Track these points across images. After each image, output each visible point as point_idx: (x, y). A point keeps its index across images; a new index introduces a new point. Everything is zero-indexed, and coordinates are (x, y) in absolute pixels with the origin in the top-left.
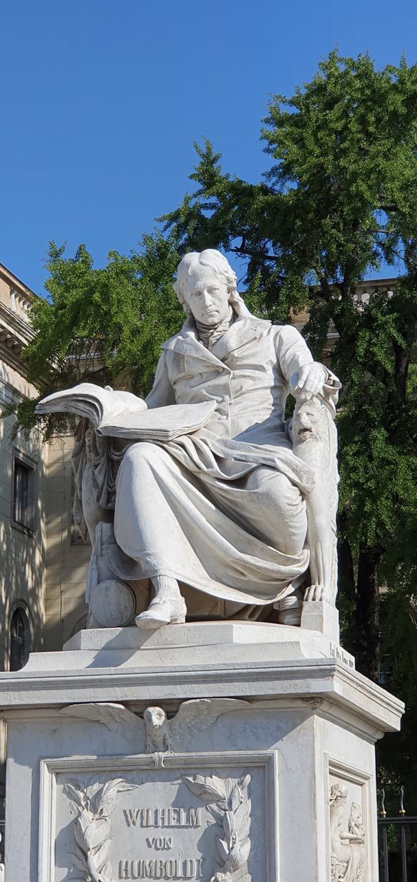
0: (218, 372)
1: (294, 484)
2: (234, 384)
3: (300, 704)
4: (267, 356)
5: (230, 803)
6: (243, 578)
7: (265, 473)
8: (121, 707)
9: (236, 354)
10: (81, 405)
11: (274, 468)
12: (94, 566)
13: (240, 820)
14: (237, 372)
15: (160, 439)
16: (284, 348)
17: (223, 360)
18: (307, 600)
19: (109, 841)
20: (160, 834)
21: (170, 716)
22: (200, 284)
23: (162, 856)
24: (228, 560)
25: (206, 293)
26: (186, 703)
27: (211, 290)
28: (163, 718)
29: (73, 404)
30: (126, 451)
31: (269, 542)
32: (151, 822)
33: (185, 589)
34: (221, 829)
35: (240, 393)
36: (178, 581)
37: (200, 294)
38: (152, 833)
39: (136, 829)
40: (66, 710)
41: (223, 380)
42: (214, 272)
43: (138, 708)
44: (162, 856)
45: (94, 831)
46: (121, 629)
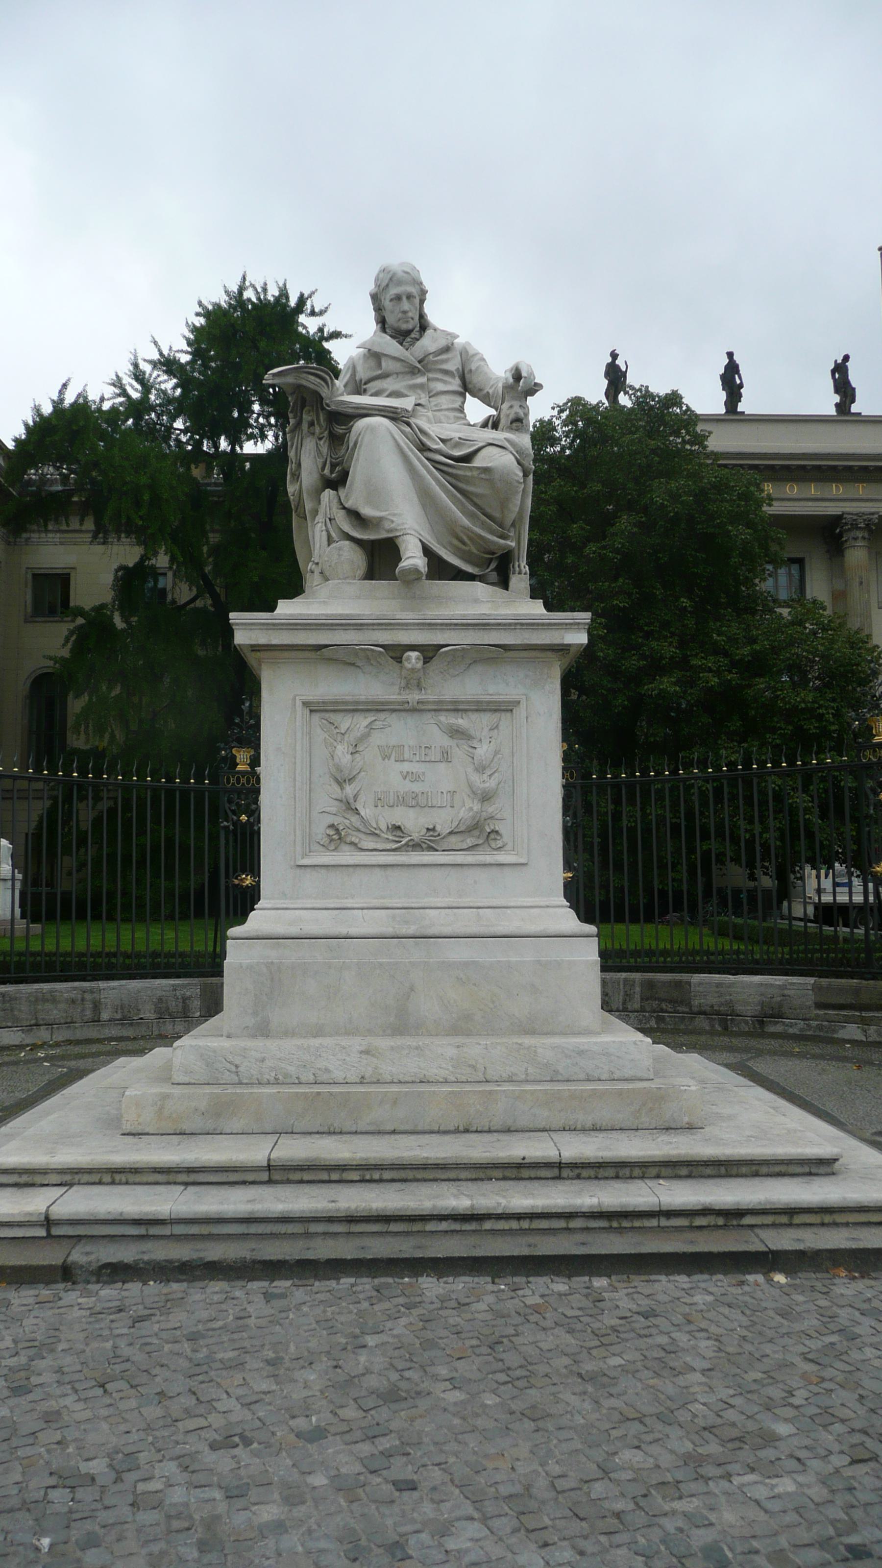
1: (519, 463)
3: (549, 654)
6: (464, 547)
8: (381, 649)
10: (312, 378)
12: (324, 528)
14: (431, 375)
17: (420, 362)
18: (514, 573)
19: (363, 773)
21: (427, 660)
25: (404, 298)
26: (444, 649)
27: (409, 297)
28: (422, 662)
29: (305, 375)
30: (352, 426)
33: (427, 551)
38: (406, 767)
43: (397, 652)
44: (416, 787)
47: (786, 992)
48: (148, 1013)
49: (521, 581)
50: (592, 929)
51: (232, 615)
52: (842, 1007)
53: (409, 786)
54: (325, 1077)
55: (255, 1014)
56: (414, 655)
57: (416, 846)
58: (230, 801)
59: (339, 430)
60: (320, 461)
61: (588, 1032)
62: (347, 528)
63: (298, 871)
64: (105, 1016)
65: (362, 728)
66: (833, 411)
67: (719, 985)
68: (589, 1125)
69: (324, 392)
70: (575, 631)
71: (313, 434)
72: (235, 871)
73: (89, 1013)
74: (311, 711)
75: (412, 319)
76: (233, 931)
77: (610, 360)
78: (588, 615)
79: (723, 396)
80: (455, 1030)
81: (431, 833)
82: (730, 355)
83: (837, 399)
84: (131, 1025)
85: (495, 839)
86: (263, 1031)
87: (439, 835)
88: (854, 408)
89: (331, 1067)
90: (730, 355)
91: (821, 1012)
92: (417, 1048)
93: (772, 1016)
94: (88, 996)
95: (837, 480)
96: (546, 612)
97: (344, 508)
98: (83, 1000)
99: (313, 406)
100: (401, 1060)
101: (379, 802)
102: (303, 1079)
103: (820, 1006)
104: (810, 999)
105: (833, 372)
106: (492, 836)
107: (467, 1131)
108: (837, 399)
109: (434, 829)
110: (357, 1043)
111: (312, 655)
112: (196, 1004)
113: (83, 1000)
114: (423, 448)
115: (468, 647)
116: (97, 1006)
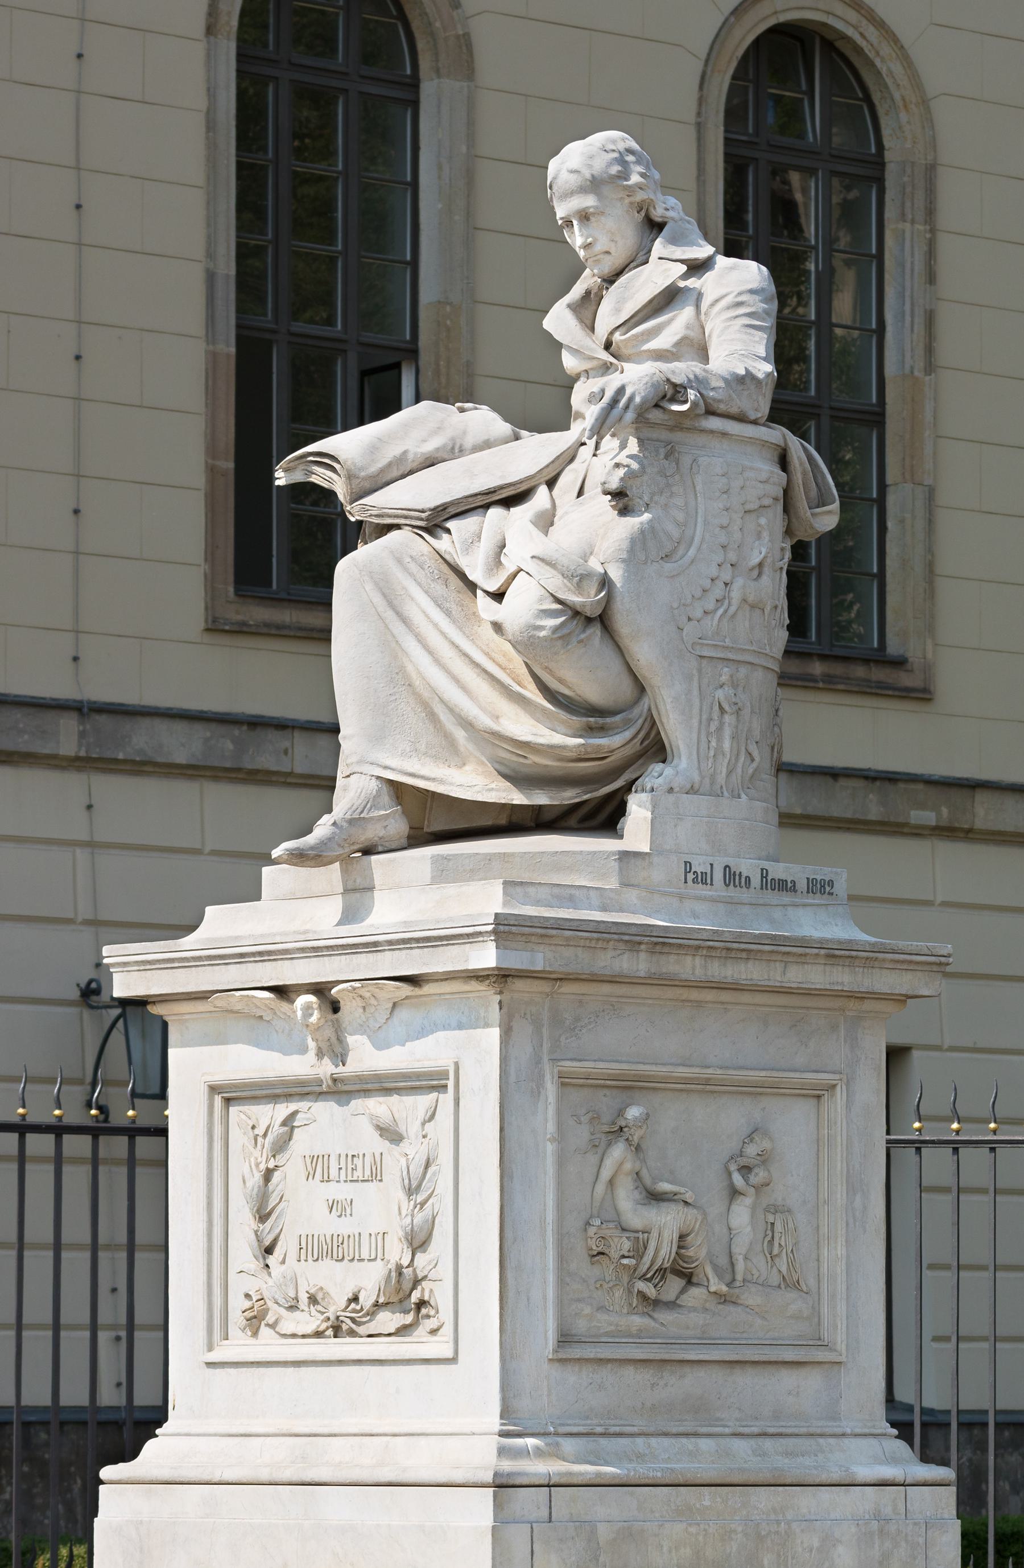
36: (391, 782)
44: (344, 1227)
51: (106, 950)
63: (211, 1371)
65: (276, 1127)
74: (228, 1101)
75: (608, 253)
81: (353, 1305)
85: (428, 1316)
87: (362, 1309)
106: (424, 1311)
109: (355, 1299)
115: (357, 984)
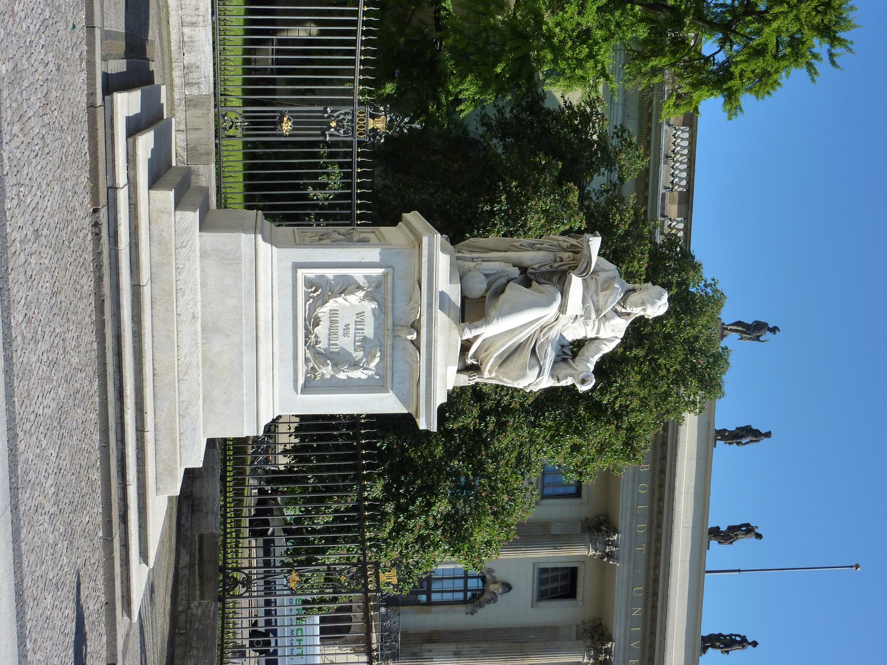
0: (598, 311)
2: (590, 322)
4: (602, 335)
5: (366, 369)
7: (536, 370)
9: (607, 323)
10: (585, 265)
11: (538, 376)
13: (358, 374)
14: (597, 322)
15: (563, 309)
16: (607, 343)
20: (352, 331)
22: (649, 306)
23: (341, 332)
24: (492, 349)
27: (644, 310)
31: (501, 365)
32: (358, 327)
33: (476, 337)
34: (355, 365)
35: (586, 324)
37: (643, 304)
38: (352, 327)
39: (354, 318)
40: (417, 286)
41: (593, 316)
42: (656, 305)
44: (341, 332)
45: (354, 299)
46: (458, 303)
47: (210, 515)
48: (188, 59)
49: (465, 380)
50: (261, 433)
52: (201, 550)
53: (341, 327)
54: (180, 295)
55: (213, 250)
56: (414, 336)
57: (308, 334)
58: (346, 114)
59: (555, 279)
60: (536, 266)
61: (204, 433)
62: (495, 286)
64: (186, 30)
66: (712, 524)
67: (213, 468)
68: (158, 438)
69: (577, 271)
70: (427, 422)
71: (556, 261)
72: (294, 117)
73: (188, 19)
76: (259, 237)
77: (771, 326)
78: (435, 430)
79: (732, 428)
80: (205, 359)
82: (768, 435)
83: (723, 528)
84: (180, 48)
86: (204, 255)
88: (714, 543)
89: (185, 297)
90: (768, 435)
91: (197, 538)
92: (197, 344)
93: (193, 505)
94: (201, 19)
95: (650, 529)
96: (438, 405)
97: (508, 282)
98: (198, 15)
99: (574, 260)
100: (189, 334)
101: (333, 313)
102: (179, 283)
103: (201, 537)
104: (205, 531)
105: (747, 525)
107: (154, 375)
108: (723, 528)
110: (199, 310)
111: (416, 278)
112: (195, 91)
113: (198, 15)
114: (542, 328)
116: (193, 24)
